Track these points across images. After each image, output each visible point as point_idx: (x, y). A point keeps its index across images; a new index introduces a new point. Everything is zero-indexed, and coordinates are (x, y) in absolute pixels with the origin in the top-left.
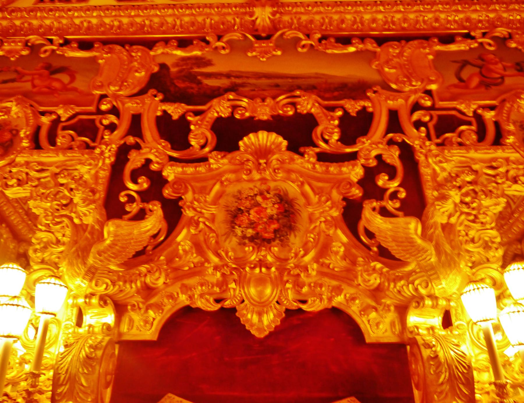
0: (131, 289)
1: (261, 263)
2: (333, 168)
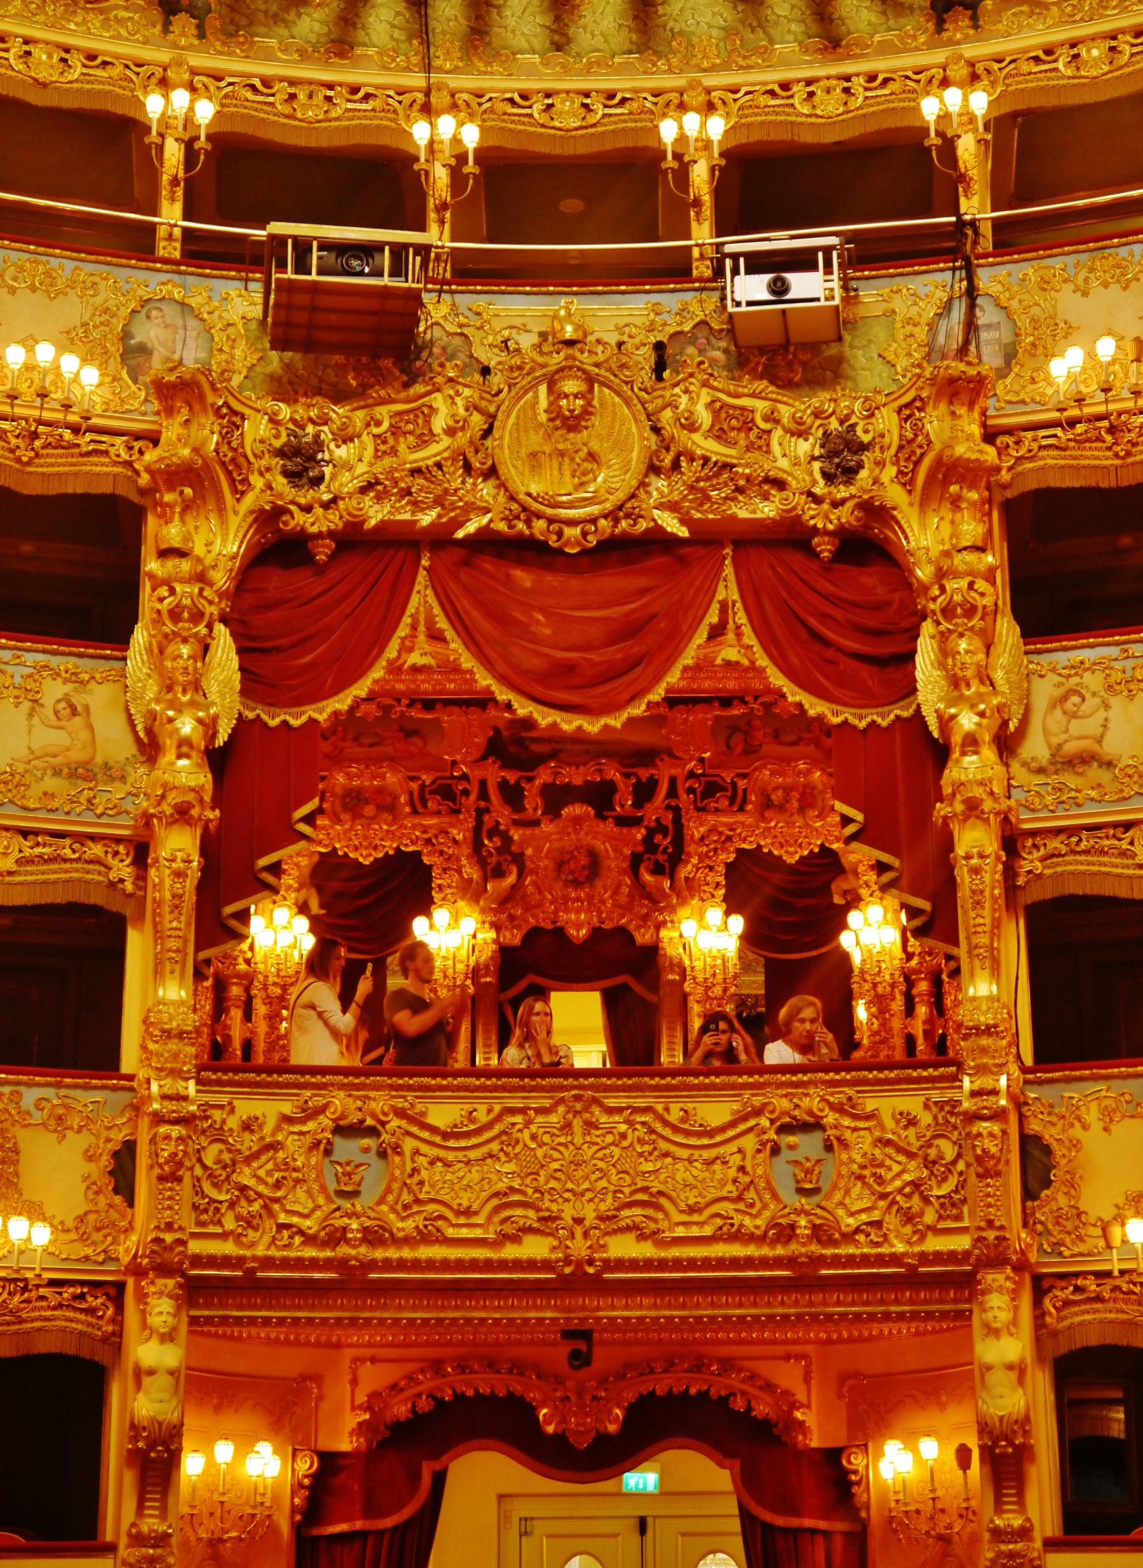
1: (578, 899)
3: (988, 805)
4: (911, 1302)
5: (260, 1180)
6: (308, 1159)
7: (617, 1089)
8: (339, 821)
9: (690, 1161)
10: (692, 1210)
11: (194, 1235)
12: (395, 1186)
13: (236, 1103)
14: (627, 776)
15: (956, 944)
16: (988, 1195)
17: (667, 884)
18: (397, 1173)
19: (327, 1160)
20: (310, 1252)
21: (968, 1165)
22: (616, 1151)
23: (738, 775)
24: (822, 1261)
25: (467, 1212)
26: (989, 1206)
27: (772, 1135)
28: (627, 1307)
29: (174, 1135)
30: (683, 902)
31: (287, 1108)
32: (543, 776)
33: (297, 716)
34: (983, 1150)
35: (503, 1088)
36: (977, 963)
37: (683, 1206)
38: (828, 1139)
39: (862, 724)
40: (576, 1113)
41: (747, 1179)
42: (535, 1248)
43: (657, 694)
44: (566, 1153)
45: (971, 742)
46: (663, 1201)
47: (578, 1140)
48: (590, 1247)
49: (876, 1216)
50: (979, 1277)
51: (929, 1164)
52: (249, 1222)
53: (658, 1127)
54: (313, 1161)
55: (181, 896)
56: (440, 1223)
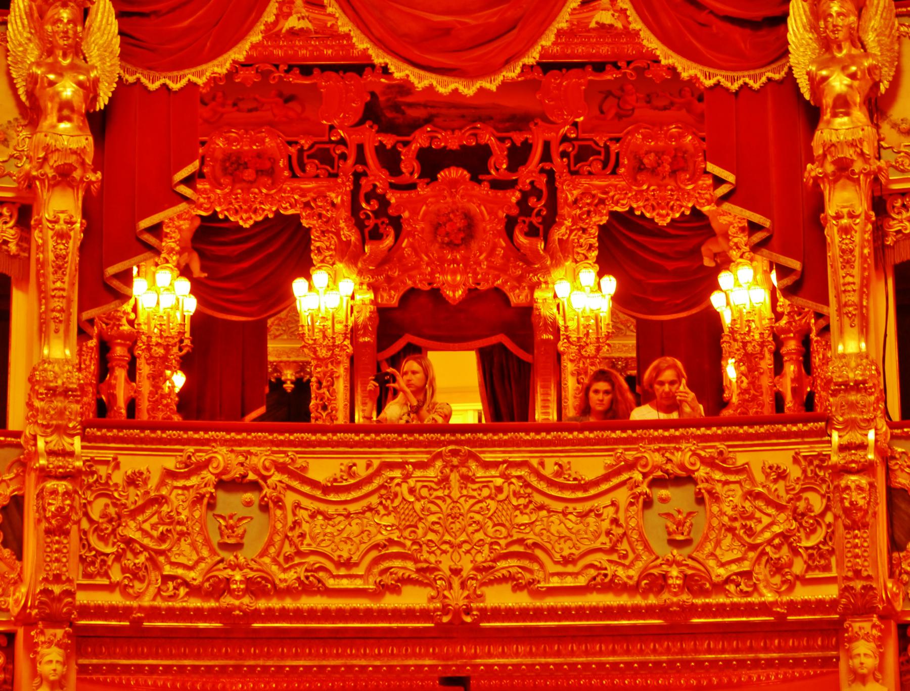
0: (381, 278)
1: (454, 261)
2: (500, 194)
3: (858, 166)
4: (779, 649)
5: (145, 533)
6: (191, 512)
7: (493, 444)
8: (220, 186)
9: (564, 514)
10: (566, 561)
11: (82, 587)
12: (277, 538)
13: (120, 458)
14: (501, 140)
15: (826, 303)
16: (856, 546)
17: (541, 246)
18: (279, 526)
19: (210, 514)
20: (195, 603)
21: (836, 517)
22: (493, 505)
23: (611, 139)
24: (693, 610)
25: (348, 564)
26: (857, 556)
27: (644, 488)
28: (503, 655)
29: (61, 490)
30: (557, 264)
31: (170, 463)
32: (420, 141)
33: (175, 80)
34: (851, 503)
35: (382, 444)
36: (846, 321)
37: (557, 557)
38: (699, 493)
39: (735, 87)
40: (453, 467)
41: (620, 531)
42: (414, 598)
43: (532, 57)
44: (444, 506)
45: (843, 104)
46: (538, 553)
47: (455, 494)
48: (467, 597)
49: (746, 566)
50: (846, 625)
51: (797, 516)
52: (135, 574)
53: (533, 480)
54: (197, 515)
55: (64, 257)
56: (321, 574)
